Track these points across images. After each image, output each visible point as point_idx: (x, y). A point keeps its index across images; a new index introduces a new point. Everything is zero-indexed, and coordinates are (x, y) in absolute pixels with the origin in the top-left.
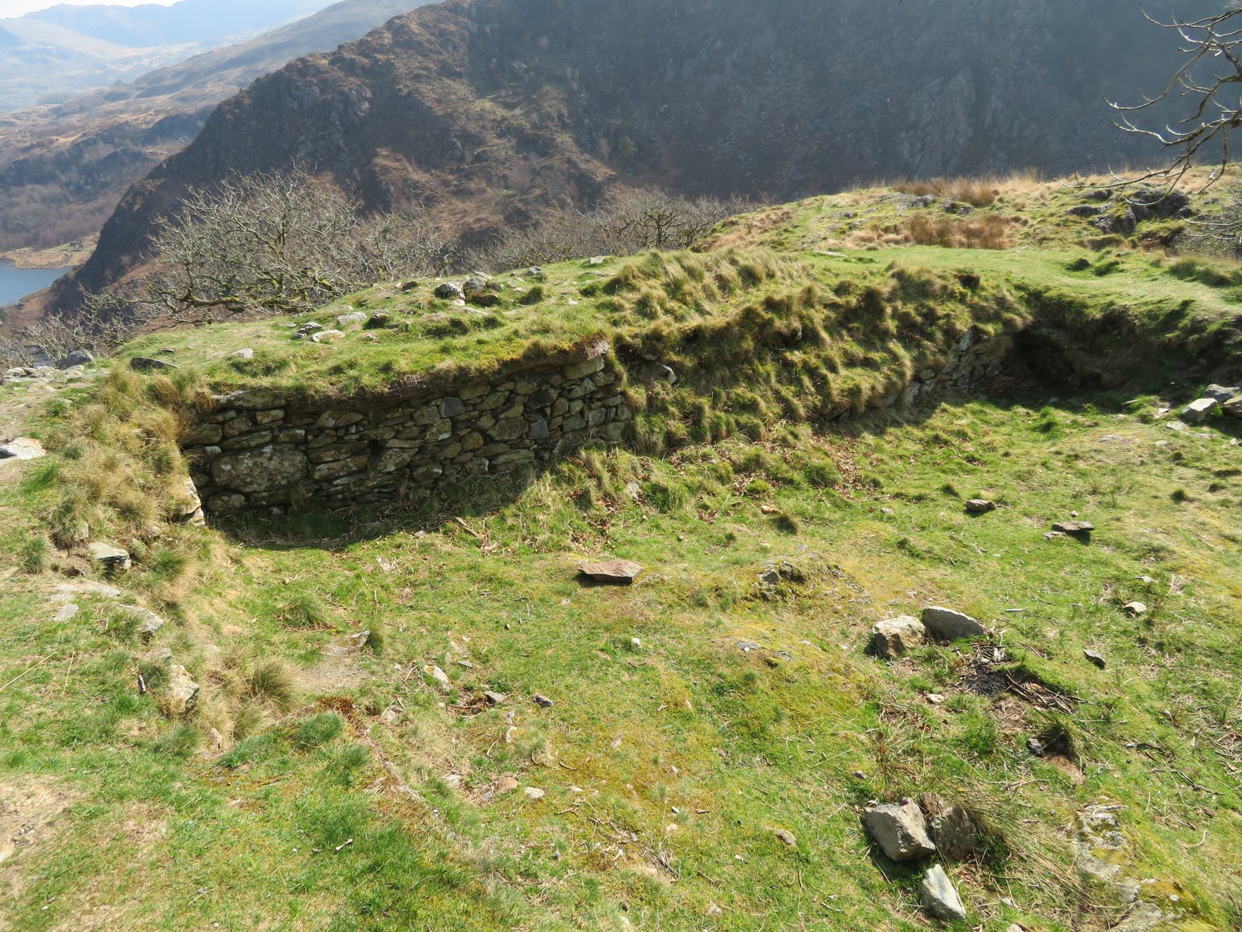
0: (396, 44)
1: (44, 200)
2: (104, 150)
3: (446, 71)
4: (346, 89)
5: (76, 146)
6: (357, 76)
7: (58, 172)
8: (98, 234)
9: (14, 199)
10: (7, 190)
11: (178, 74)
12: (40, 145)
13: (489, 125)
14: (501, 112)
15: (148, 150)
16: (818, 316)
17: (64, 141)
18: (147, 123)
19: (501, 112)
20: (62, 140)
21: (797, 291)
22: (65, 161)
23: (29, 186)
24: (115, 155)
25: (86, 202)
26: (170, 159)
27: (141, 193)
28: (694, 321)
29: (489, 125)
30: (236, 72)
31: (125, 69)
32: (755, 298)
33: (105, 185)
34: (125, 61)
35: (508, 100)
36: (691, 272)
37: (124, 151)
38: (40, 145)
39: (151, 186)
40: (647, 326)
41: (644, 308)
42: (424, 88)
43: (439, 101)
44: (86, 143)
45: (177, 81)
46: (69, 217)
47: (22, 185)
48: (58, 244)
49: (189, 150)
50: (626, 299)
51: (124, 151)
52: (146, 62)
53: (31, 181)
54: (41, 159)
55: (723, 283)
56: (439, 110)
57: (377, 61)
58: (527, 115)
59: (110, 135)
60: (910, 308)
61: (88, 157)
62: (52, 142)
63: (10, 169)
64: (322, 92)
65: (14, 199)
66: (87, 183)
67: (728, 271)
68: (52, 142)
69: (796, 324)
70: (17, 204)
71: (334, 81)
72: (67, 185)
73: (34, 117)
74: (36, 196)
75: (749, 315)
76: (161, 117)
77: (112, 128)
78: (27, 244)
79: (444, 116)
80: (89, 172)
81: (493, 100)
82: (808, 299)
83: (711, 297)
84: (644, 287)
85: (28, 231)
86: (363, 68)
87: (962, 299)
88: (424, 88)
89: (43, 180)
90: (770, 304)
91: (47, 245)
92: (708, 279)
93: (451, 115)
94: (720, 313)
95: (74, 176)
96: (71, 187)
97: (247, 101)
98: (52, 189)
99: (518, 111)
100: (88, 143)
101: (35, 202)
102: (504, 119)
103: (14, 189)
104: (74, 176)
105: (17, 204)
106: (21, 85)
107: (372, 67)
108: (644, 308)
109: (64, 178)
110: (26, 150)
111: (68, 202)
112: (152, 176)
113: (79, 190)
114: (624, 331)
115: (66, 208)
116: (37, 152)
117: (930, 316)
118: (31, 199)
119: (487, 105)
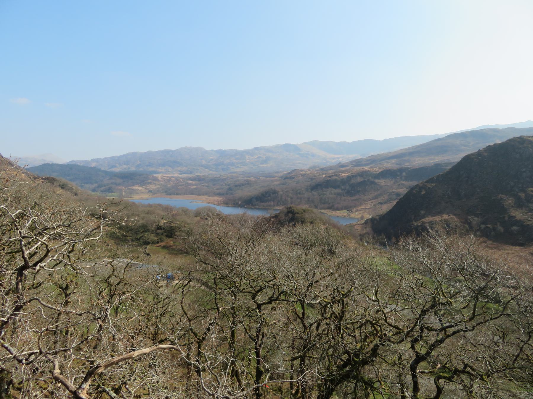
2: (359, 179)
5: (349, 178)
8: (395, 203)
9: (325, 192)
11: (368, 160)
12: (336, 175)
15: (377, 181)
17: (344, 175)
20: (343, 175)
22: (344, 182)
24: (364, 181)
30: (394, 161)
31: (333, 161)
33: (359, 192)
34: (334, 159)
37: (368, 180)
38: (335, 175)
44: (353, 176)
45: (368, 162)
46: (344, 200)
47: (328, 188)
48: (342, 210)
51: (368, 180)
52: (341, 159)
54: (336, 180)
59: (362, 174)
61: (353, 181)
65: (325, 192)
70: (326, 194)
72: (344, 190)
73: (314, 170)
74: (332, 192)
76: (380, 170)
78: (329, 208)
85: (329, 204)
89: (335, 187)
91: (338, 209)
95: (348, 187)
100: (354, 176)
101: (332, 194)
103: (324, 189)
104: (348, 187)
110: (330, 177)
115: (343, 198)
116: (334, 178)
118: (331, 193)
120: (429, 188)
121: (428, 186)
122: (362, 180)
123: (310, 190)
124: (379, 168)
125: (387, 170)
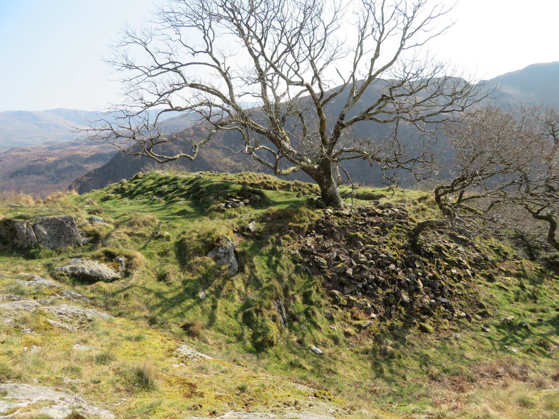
0: (195, 134)
1: (37, 182)
2: (67, 164)
3: (214, 146)
4: (172, 149)
5: (56, 162)
6: (177, 145)
7: (46, 171)
10: (22, 176)
12: (41, 160)
13: (228, 168)
14: (233, 163)
15: (85, 166)
16: (277, 186)
17: (51, 159)
18: (87, 155)
19: (233, 163)
20: (50, 159)
21: (273, 181)
22: (49, 167)
23: (32, 176)
24: (71, 167)
25: (54, 184)
26: (95, 170)
27: (81, 182)
28: (253, 182)
29: (228, 168)
32: (265, 181)
33: (64, 178)
35: (237, 159)
36: (254, 175)
37: (75, 166)
38: (41, 160)
39: (85, 179)
40: (244, 181)
41: (244, 179)
42: (203, 152)
43: (209, 157)
47: (29, 175)
49: (104, 167)
50: (241, 178)
53: (34, 174)
54: (40, 166)
55: (260, 178)
56: (209, 161)
57: (186, 140)
58: (244, 165)
59: (70, 159)
60: (296, 188)
61: (59, 166)
62: (46, 159)
63: (26, 168)
64: (163, 149)
65: (25, 180)
66: (57, 176)
67: (261, 176)
68: (46, 159)
69: (272, 186)
70: (26, 182)
71: (168, 146)
72: (48, 176)
75: (262, 182)
76: (93, 154)
77: (72, 156)
79: (210, 163)
80: (58, 172)
81: (231, 158)
82: (276, 183)
83: (257, 180)
84: (245, 176)
86: (180, 142)
87: (308, 188)
88: (203, 152)
89: (38, 174)
90: (267, 182)
92: (257, 177)
93: (213, 163)
94: (257, 182)
95: (52, 173)
96: (50, 178)
97: (131, 150)
98: (41, 178)
99: (240, 164)
100: (61, 161)
101: (33, 182)
102: (234, 166)
103: (25, 176)
104: (52, 173)
105: (26, 182)
106: (37, 136)
107: (184, 142)
108: (244, 179)
109: (47, 174)
110: (35, 161)
111: (47, 183)
112: (86, 175)
113: (53, 179)
114: (240, 181)
116: (39, 162)
117: (300, 190)
119: (228, 160)
120: (84, 182)
121: (84, 180)
122: (69, 164)
123: (7, 178)
124: (92, 152)
125: (98, 154)
